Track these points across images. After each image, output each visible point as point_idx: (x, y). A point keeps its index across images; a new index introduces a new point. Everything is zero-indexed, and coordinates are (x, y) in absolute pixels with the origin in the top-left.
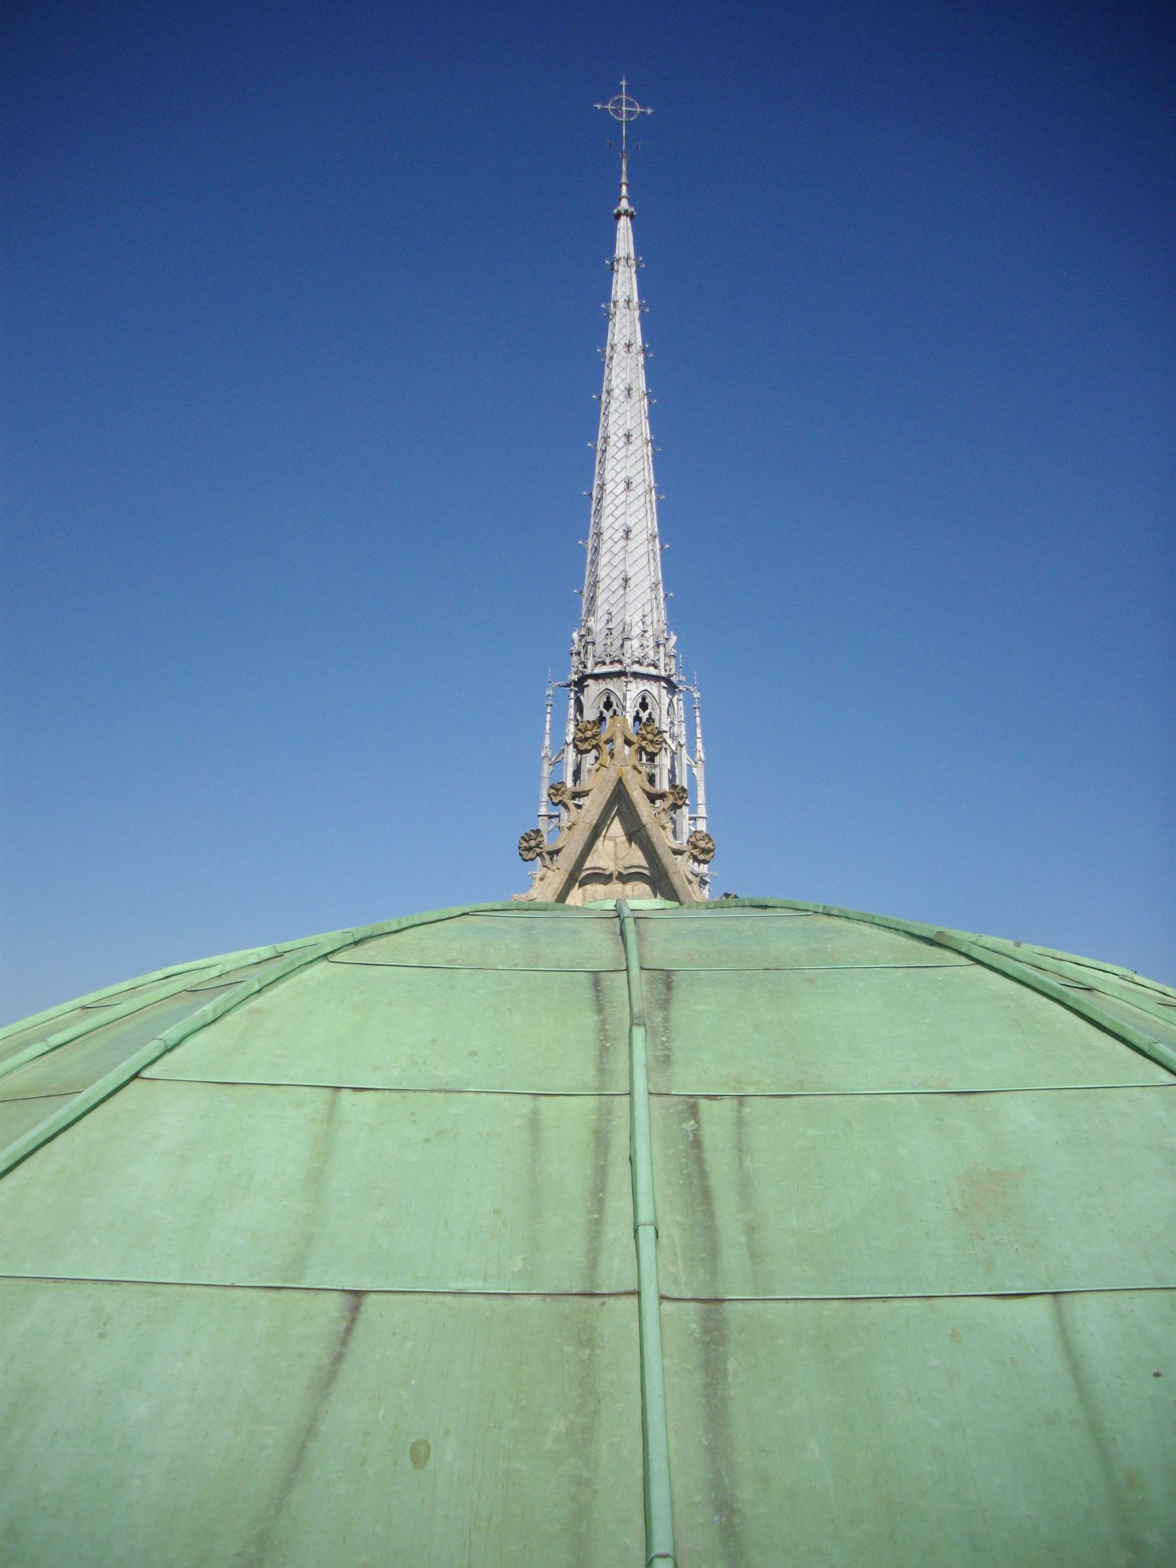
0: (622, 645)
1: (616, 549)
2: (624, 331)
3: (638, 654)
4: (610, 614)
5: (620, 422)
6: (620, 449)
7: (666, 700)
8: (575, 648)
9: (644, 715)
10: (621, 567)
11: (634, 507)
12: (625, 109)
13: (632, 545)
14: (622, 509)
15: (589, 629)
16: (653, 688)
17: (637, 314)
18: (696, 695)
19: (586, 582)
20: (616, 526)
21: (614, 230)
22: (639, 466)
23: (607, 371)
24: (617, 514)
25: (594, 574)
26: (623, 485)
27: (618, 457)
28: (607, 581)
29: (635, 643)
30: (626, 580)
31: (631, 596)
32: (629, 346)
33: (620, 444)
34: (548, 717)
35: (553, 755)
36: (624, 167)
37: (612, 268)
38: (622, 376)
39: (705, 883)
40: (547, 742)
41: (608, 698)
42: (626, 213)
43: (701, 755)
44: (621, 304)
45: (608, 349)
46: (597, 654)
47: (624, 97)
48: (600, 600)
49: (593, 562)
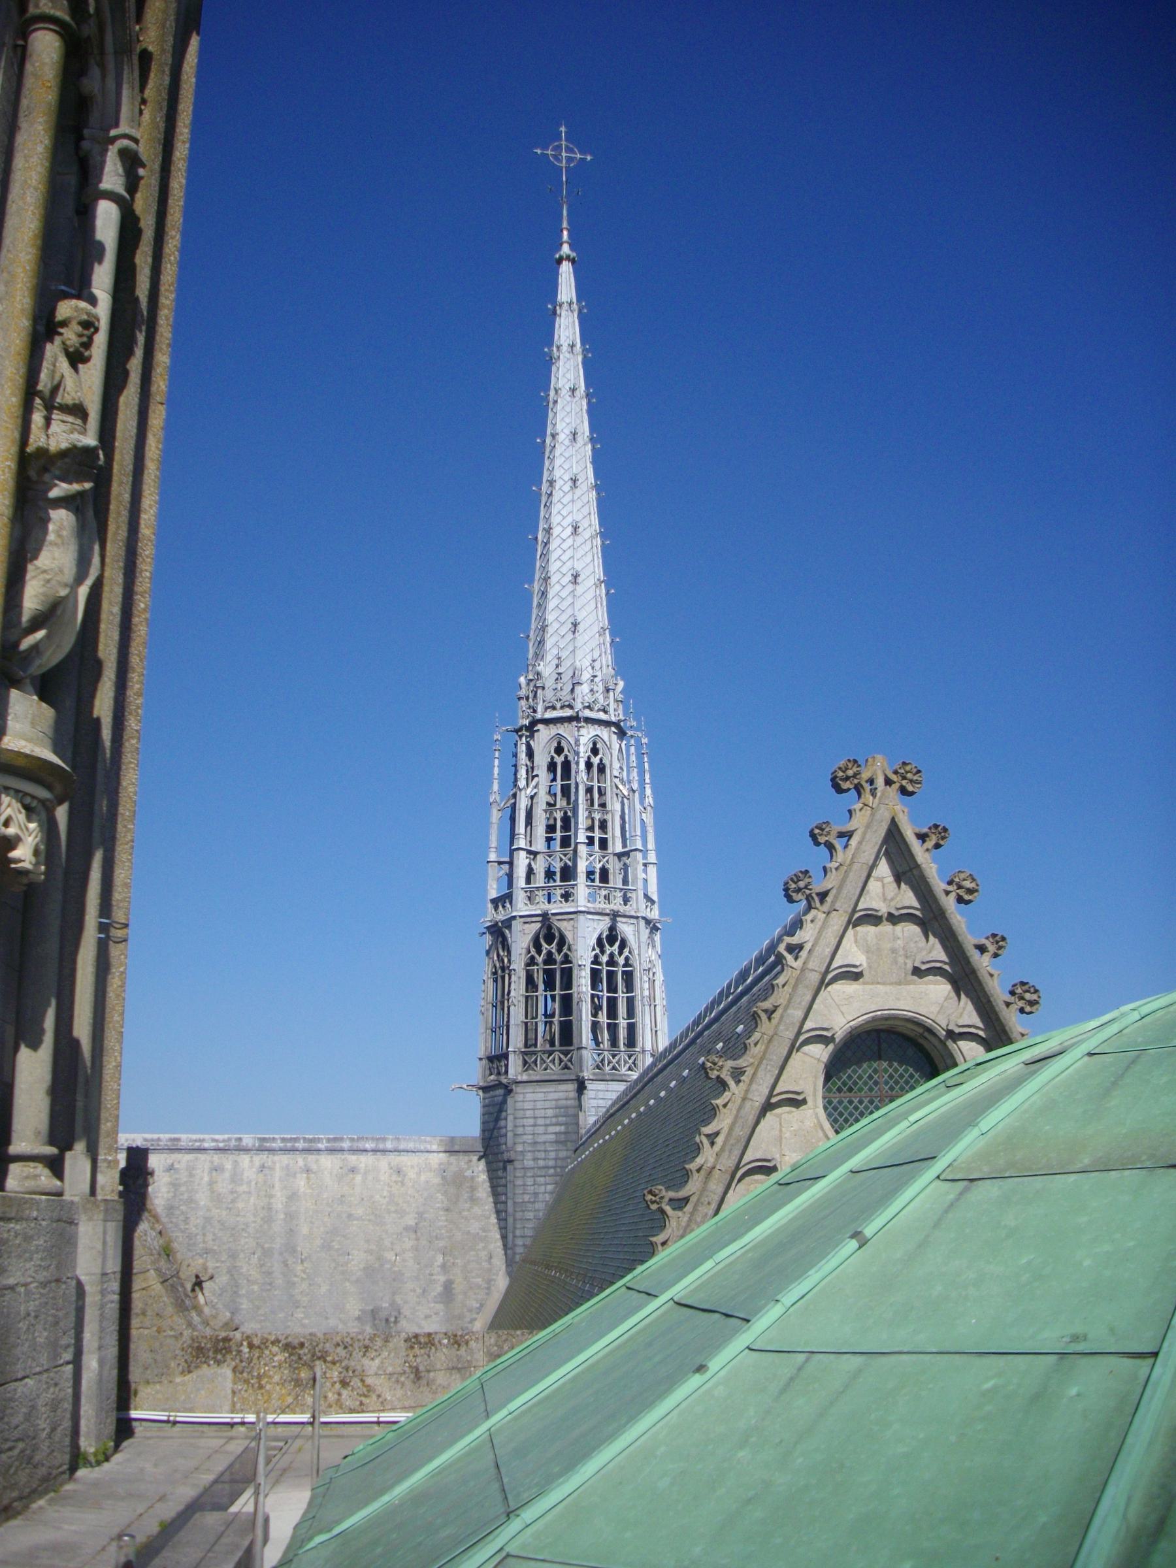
0: (572, 690)
1: (564, 594)
2: (568, 376)
3: (589, 699)
4: (559, 658)
6: (566, 494)
7: (616, 746)
8: (523, 693)
9: (596, 761)
10: (570, 612)
11: (581, 552)
12: (565, 155)
13: (580, 589)
14: (569, 554)
15: (538, 674)
17: (580, 358)
18: (645, 740)
19: (533, 627)
20: (564, 570)
21: (557, 274)
22: (585, 511)
23: (551, 415)
24: (564, 558)
25: (542, 618)
26: (569, 530)
27: (565, 501)
28: (556, 625)
29: (585, 688)
30: (575, 625)
32: (573, 390)
33: (567, 488)
34: (496, 762)
36: (565, 212)
37: (554, 312)
38: (567, 420)
39: (657, 929)
40: (496, 787)
41: (559, 743)
42: (568, 258)
43: (650, 800)
44: (565, 348)
45: (552, 393)
46: (547, 699)
47: (564, 143)
48: (549, 643)
49: (539, 605)
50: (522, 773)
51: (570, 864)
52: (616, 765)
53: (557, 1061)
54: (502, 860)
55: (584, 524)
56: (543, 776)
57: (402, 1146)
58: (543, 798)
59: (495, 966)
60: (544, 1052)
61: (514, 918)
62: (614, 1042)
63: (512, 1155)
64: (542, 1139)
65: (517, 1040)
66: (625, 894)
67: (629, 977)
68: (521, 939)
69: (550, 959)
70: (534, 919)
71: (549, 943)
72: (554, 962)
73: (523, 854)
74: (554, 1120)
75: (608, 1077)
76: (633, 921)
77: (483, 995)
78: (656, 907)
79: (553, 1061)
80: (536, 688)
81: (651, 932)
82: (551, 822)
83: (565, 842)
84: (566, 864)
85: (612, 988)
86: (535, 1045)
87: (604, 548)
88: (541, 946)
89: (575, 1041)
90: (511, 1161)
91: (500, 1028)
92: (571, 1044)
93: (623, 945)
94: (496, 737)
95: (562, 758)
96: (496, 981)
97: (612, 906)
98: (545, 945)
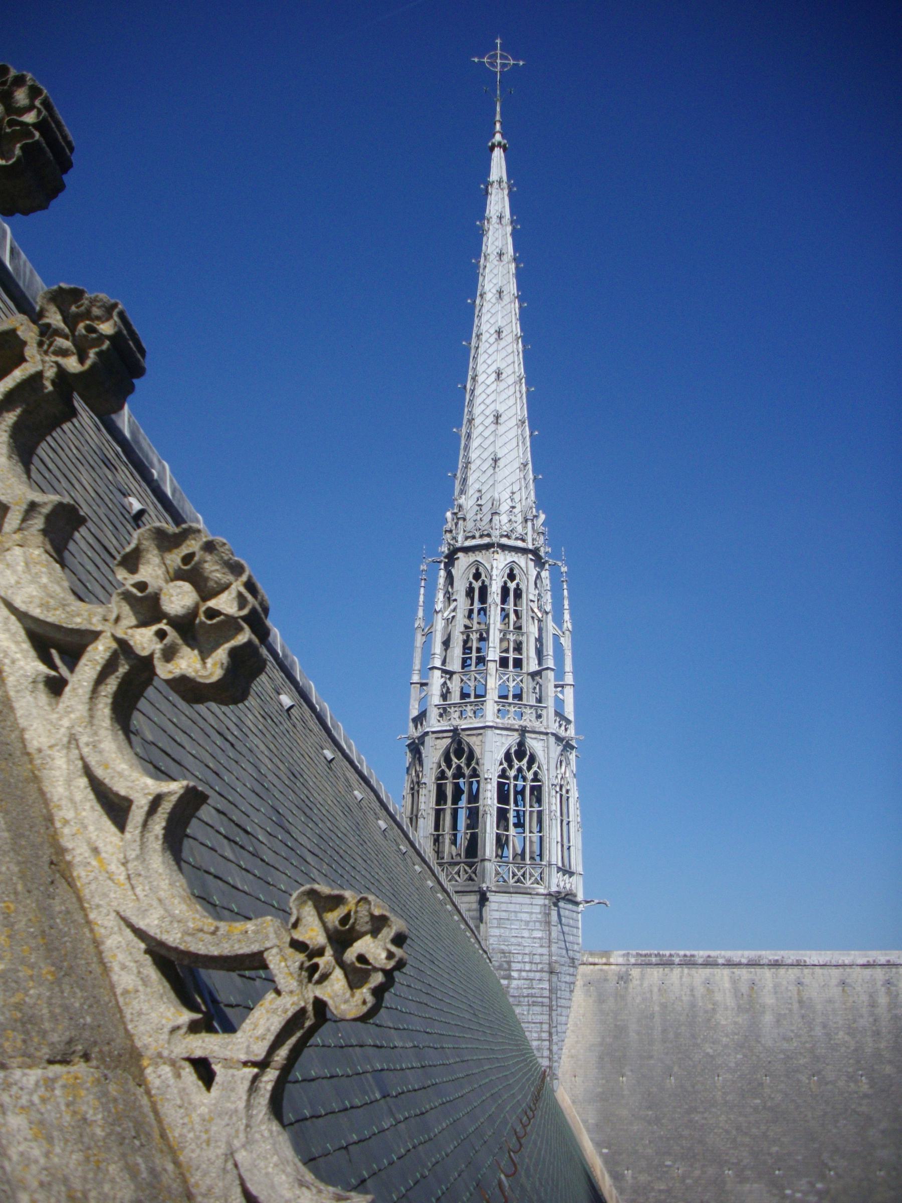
0: (491, 520)
1: (486, 434)
2: (496, 243)
3: (506, 528)
5: (492, 321)
6: (491, 345)
7: (533, 572)
8: (449, 526)
9: (512, 586)
10: (491, 449)
11: (504, 396)
12: (499, 61)
13: (502, 429)
15: (460, 507)
17: (509, 229)
18: (564, 569)
19: (460, 466)
21: (489, 160)
22: (510, 359)
23: (481, 278)
24: (488, 402)
25: (466, 457)
26: (494, 376)
27: (490, 351)
28: (478, 462)
30: (496, 460)
31: (500, 474)
33: (492, 340)
34: (422, 591)
35: (426, 626)
36: (498, 109)
37: (487, 193)
38: (494, 281)
39: (572, 748)
41: (477, 569)
42: (499, 145)
43: (568, 625)
44: (494, 220)
46: (468, 529)
48: (470, 481)
50: (440, 596)
58: (461, 620)
59: (413, 781)
61: (427, 733)
69: (459, 774)
70: (445, 735)
73: (438, 673)
75: (511, 890)
76: (542, 737)
79: (458, 873)
80: (459, 518)
88: (451, 760)
92: (475, 856)
93: (532, 760)
94: (422, 568)
95: (480, 583)
96: (413, 794)
97: (522, 723)
98: (455, 760)
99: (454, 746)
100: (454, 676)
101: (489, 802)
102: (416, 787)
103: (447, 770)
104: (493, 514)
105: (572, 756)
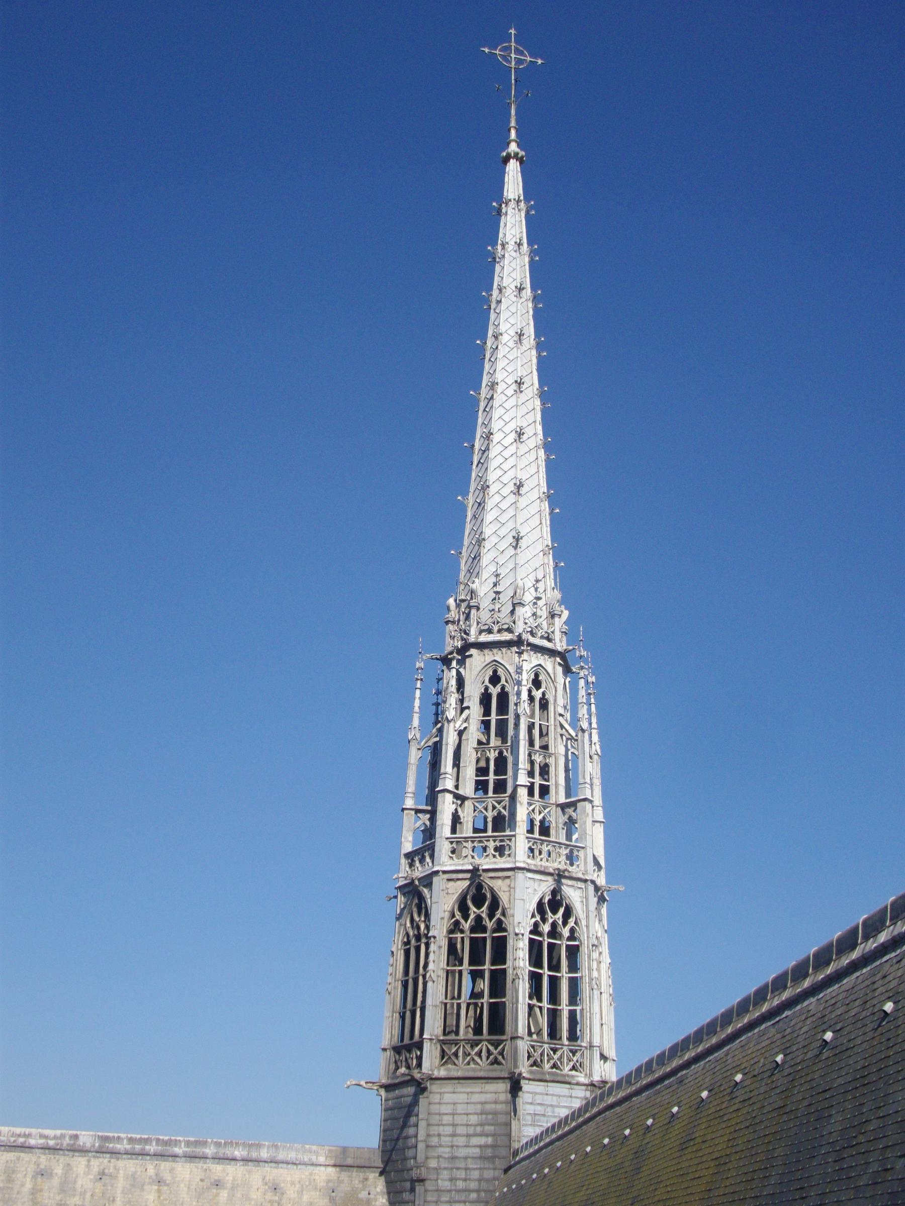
0: (512, 612)
1: (504, 506)
2: (514, 275)
3: (531, 622)
4: (497, 576)
5: (510, 369)
9: (538, 694)
10: (511, 525)
11: (524, 462)
12: (514, 57)
13: (523, 502)
14: (511, 462)
15: (472, 592)
16: (550, 665)
19: (466, 543)
20: (505, 479)
21: (503, 173)
22: (530, 418)
23: (493, 316)
24: (506, 466)
26: (513, 436)
27: (507, 405)
29: (524, 612)
30: (517, 539)
31: (522, 558)
32: (520, 289)
33: (510, 392)
34: (418, 693)
35: (422, 738)
36: (513, 112)
37: (499, 212)
38: (512, 321)
40: (416, 722)
41: (495, 672)
42: (516, 156)
44: (511, 247)
45: (495, 293)
46: (483, 620)
47: (513, 44)
48: (485, 560)
51: (505, 813)
52: (561, 701)
53: (484, 1054)
54: (420, 807)
55: (529, 432)
56: (475, 711)
57: (281, 1156)
58: (474, 733)
60: (468, 1041)
61: (437, 872)
62: (554, 1033)
63: (423, 1173)
64: (462, 1152)
65: (433, 1025)
66: (571, 852)
67: (573, 952)
68: (443, 900)
69: (479, 926)
70: (461, 876)
71: (479, 906)
72: (484, 929)
73: (449, 797)
74: (479, 1129)
75: (548, 1077)
76: (580, 884)
77: (390, 970)
78: (603, 872)
79: (479, 1054)
80: (469, 607)
81: (598, 903)
82: (483, 764)
83: (500, 787)
84: (500, 813)
85: (555, 966)
86: (457, 1033)
87: (548, 462)
88: (468, 909)
89: (508, 1028)
90: (422, 1181)
91: (411, 1008)
92: (503, 1032)
95: (498, 689)
97: (556, 865)
98: (473, 909)
99: (473, 891)
100: (466, 802)
101: (522, 964)
102: (413, 942)
103: (462, 921)
104: (514, 605)
105: (604, 911)
